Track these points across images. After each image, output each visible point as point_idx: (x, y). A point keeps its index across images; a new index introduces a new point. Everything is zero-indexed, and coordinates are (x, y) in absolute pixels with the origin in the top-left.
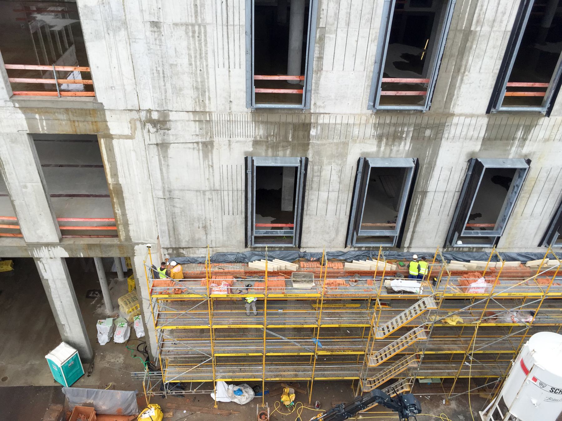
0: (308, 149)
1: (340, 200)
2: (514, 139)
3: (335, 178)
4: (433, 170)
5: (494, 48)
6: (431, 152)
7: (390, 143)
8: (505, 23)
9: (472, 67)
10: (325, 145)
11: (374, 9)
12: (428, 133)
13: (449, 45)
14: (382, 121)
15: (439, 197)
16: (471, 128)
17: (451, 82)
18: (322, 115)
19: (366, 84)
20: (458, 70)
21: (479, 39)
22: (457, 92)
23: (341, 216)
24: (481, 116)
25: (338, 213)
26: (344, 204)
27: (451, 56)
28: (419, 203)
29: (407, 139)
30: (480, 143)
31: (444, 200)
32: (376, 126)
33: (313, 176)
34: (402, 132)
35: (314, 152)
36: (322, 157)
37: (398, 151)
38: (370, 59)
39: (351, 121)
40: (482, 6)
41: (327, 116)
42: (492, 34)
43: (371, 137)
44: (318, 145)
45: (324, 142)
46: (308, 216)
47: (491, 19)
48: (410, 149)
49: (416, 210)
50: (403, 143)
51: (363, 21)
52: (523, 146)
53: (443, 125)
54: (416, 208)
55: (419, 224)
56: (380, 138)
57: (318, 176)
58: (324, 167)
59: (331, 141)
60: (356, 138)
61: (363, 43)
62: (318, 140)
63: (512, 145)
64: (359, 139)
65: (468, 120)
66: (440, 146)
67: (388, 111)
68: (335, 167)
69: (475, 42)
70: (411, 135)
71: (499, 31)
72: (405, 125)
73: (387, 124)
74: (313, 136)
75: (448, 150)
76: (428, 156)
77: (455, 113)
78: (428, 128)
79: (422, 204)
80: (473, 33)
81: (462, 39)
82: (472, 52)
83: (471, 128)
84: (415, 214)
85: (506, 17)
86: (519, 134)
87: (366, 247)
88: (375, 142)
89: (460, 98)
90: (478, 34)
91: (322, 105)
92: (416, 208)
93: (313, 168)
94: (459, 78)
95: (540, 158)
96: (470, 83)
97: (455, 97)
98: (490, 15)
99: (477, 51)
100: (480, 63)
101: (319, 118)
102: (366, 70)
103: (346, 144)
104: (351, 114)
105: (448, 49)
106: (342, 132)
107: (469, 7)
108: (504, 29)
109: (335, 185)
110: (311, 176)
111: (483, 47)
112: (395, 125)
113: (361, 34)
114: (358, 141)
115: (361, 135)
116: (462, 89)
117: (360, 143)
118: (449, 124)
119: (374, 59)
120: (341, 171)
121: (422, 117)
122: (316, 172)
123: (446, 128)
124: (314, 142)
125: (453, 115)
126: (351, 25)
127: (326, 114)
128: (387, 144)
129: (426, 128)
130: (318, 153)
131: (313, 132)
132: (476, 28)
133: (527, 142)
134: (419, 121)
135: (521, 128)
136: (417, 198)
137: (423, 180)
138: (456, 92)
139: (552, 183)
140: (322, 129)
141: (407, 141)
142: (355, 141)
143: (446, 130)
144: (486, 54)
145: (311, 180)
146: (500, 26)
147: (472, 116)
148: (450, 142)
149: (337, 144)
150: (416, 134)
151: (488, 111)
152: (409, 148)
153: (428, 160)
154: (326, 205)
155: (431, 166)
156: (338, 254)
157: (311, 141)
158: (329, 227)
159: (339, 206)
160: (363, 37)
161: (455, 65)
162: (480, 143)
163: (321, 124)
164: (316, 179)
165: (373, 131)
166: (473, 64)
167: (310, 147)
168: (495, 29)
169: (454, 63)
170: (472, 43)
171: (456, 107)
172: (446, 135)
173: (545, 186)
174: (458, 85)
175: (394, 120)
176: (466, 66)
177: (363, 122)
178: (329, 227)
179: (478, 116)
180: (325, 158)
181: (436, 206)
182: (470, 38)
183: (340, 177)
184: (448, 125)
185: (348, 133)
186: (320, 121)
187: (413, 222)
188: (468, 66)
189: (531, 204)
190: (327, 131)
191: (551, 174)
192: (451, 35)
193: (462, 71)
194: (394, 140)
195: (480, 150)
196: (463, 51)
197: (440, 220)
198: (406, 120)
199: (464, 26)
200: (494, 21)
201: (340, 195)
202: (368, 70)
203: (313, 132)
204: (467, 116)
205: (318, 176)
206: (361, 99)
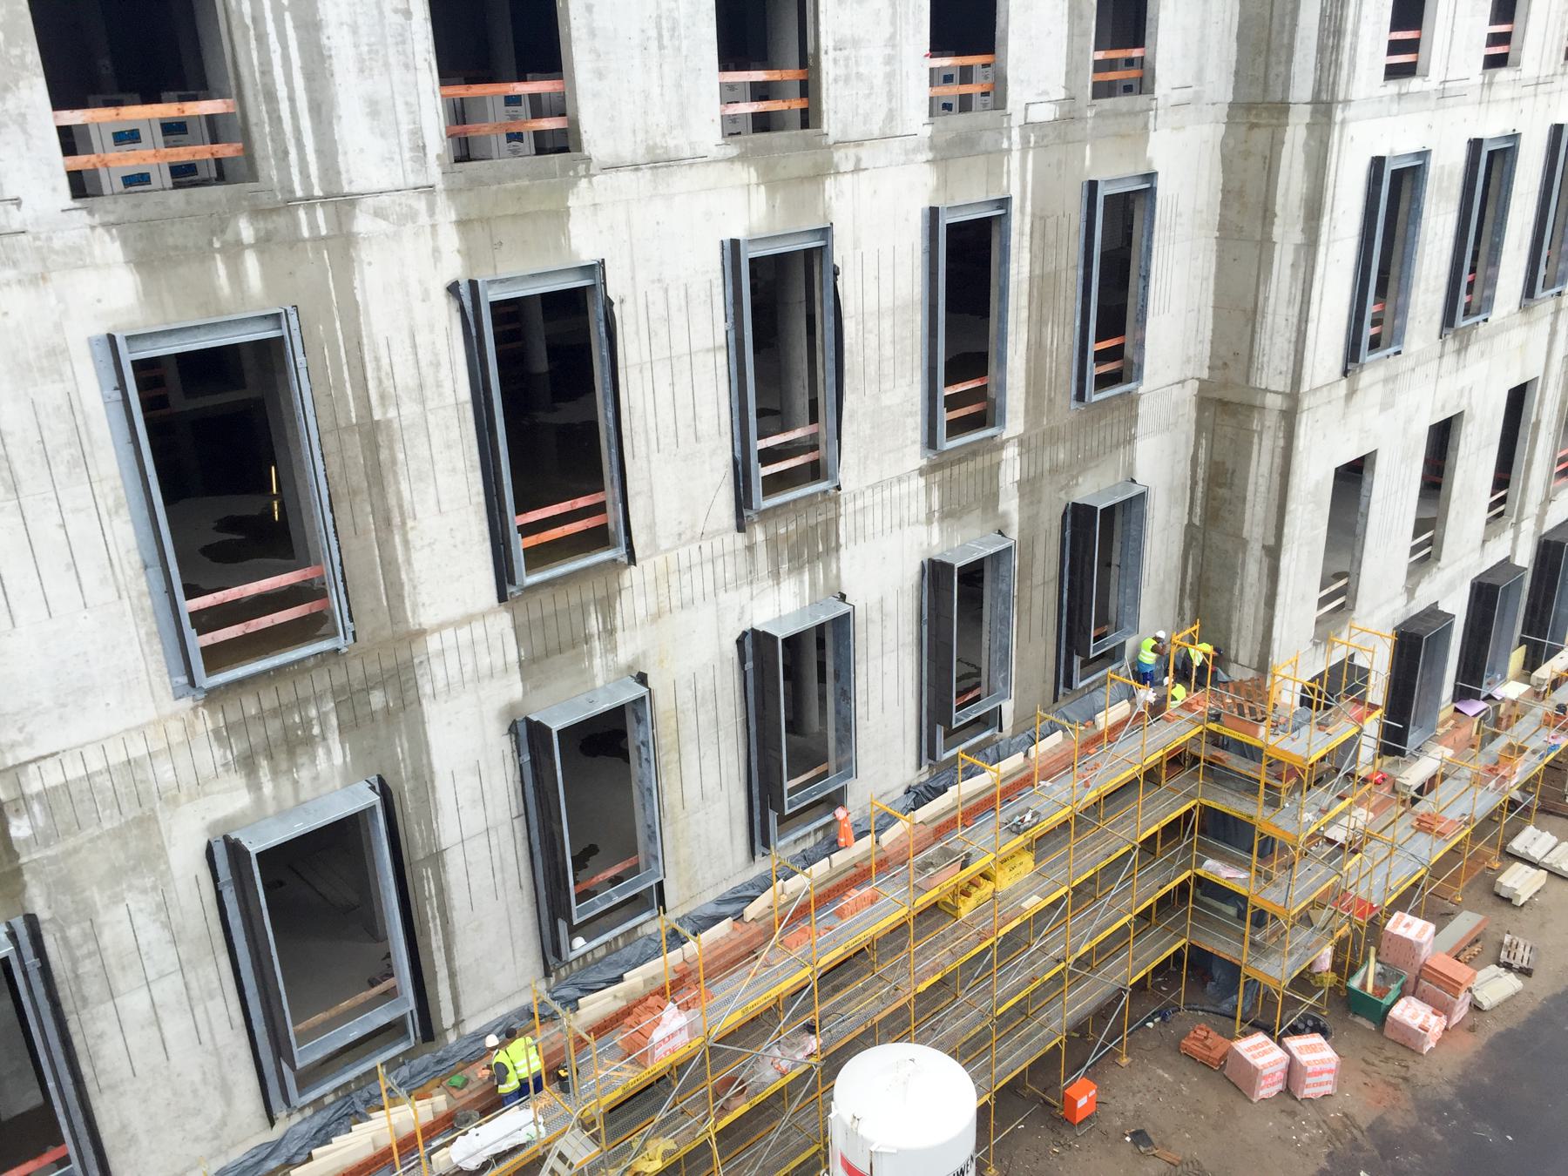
0: (24, 886)
1: (195, 992)
2: (587, 639)
3: (152, 934)
4: (433, 787)
5: (449, 447)
6: (406, 745)
7: (284, 766)
8: (448, 385)
9: (417, 507)
10: (76, 850)
11: (82, 429)
12: (377, 699)
13: (334, 469)
14: (233, 716)
15: (478, 848)
16: (481, 649)
17: (380, 556)
18: (32, 768)
19: (143, 632)
20: (385, 522)
21: (405, 437)
22: (408, 574)
23: (218, 1038)
24: (491, 611)
25: (205, 1036)
26: (212, 997)
27: (353, 492)
28: (433, 892)
29: (329, 735)
30: (517, 677)
31: (495, 853)
32: (221, 736)
33: (75, 962)
34: (306, 724)
35: (48, 886)
36: (83, 891)
37: (316, 778)
38: (126, 566)
39: (138, 750)
40: (377, 359)
41: (48, 764)
42: (431, 418)
43: (220, 769)
44: (53, 860)
45: (71, 842)
46: (107, 1096)
47: (412, 383)
48: (348, 759)
49: (433, 913)
50: (321, 752)
51: (60, 470)
52: (614, 649)
53: (409, 666)
54: (432, 908)
55: (459, 946)
56: (247, 764)
57: (90, 955)
58: (104, 918)
59: (93, 831)
60: (175, 792)
61: (83, 527)
62: (47, 846)
63: (591, 655)
64: (184, 790)
65: (464, 633)
66: (423, 723)
67: (240, 683)
68: (140, 904)
69: (398, 447)
70: (334, 721)
71: (444, 407)
72: (307, 700)
73: (254, 717)
74: (26, 840)
75: (449, 724)
76: (404, 760)
77: (424, 626)
78: (372, 688)
79: (441, 890)
80: (382, 427)
81: (362, 447)
82: (401, 470)
83: (481, 649)
84: (435, 925)
85: (445, 372)
86: (594, 624)
87: (336, 1090)
88: (238, 780)
90: (396, 425)
91: (20, 737)
92: (432, 908)
93: (65, 939)
94: (397, 539)
95: (661, 661)
96: (430, 545)
97: (407, 588)
98: (404, 376)
99: (413, 465)
100: (432, 490)
101: (23, 779)
102: (124, 594)
103: (146, 823)
104: (127, 730)
105: (337, 478)
106: (121, 790)
107: (345, 368)
108: (452, 401)
109: (163, 956)
110: (68, 965)
111: (423, 451)
112: (277, 712)
113: (66, 505)
114: (183, 798)
115: (187, 776)
116: (416, 566)
117: (191, 799)
118: (423, 658)
119: (136, 558)
120: (164, 906)
121: (343, 666)
122: (79, 946)
123: (419, 672)
124: (36, 856)
125: (421, 633)
126: (25, 489)
127: (44, 758)
128: (275, 773)
129: (367, 690)
130: (64, 884)
131: (19, 829)
132: (385, 413)
133: (619, 635)
134: (339, 678)
135: (592, 609)
136: (422, 879)
137: (419, 824)
138: (404, 576)
140: (50, 811)
141: (330, 742)
142: (174, 802)
143: (422, 676)
145: (70, 975)
146: (440, 395)
147: (469, 619)
148: (446, 702)
149: (118, 834)
150: (346, 716)
151: (502, 597)
152: (345, 756)
153: (410, 769)
154: (155, 1028)
155: (424, 780)
156: (255, 1159)
157: (23, 860)
158: (195, 1092)
159: (199, 1011)
160: (76, 511)
161: (373, 512)
162: (516, 677)
163: (38, 796)
164: (87, 967)
165: (218, 752)
167: (27, 877)
168: (430, 405)
169: (369, 509)
170: (391, 449)
171: (422, 610)
172: (426, 689)
174: (401, 558)
175: (269, 701)
176: (401, 507)
177: (176, 736)
178: (195, 1092)
180: (95, 889)
181: (481, 877)
182: (382, 439)
183: (167, 925)
184: (421, 662)
185: (140, 787)
186: (33, 786)
187: (439, 948)
188: (407, 506)
189: (691, 772)
190: (69, 809)
191: (699, 687)
192: (331, 443)
193: (396, 520)
194: (291, 753)
195: (525, 693)
196: (377, 476)
197: (507, 909)
198: (304, 687)
199: (353, 415)
200: (421, 386)
201: (190, 976)
202: (134, 594)
203: (19, 828)
204: (457, 624)
205: (90, 955)
206: (145, 678)
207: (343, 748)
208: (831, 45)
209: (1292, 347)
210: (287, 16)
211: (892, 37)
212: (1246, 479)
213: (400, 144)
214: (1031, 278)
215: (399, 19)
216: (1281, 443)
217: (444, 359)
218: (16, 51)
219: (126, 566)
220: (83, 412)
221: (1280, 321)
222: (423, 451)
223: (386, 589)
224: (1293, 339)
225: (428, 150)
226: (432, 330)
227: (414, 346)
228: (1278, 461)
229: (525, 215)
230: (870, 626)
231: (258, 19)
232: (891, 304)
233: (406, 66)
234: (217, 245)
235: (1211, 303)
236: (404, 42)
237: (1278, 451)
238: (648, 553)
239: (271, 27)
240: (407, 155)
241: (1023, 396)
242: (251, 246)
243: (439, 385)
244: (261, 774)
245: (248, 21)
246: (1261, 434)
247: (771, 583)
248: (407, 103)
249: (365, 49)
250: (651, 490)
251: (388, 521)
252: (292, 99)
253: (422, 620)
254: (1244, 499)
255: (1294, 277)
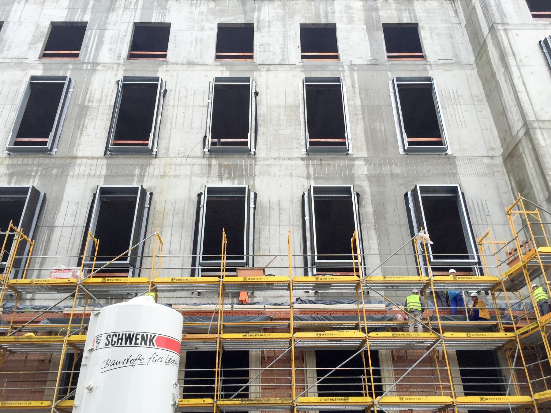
5: (103, 114)
6: (57, 188)
9: (88, 126)
12: (55, 171)
13: (69, 112)
15: (67, 232)
16: (94, 168)
19: (4, 137)
22: (78, 141)
24: (101, 158)
28: (45, 240)
30: (103, 179)
31: (73, 236)
34: (31, 171)
42: (101, 107)
48: (38, 185)
49: (42, 248)
50: (32, 180)
54: (42, 246)
65: (90, 161)
70: (39, 173)
75: (74, 186)
77: (77, 156)
78: (55, 168)
82: (87, 116)
83: (94, 168)
84: (41, 253)
85: (109, 98)
89: (81, 146)
90: (90, 107)
92: (42, 246)
95: (161, 192)
96: (88, 136)
98: (97, 97)
100: (94, 123)
102: (6, 128)
116: (82, 140)
125: (76, 158)
129: (53, 168)
133: (145, 178)
139: (181, 216)
143: (71, 169)
144: (98, 118)
147: (92, 158)
148: (76, 179)
152: (38, 184)
166: (88, 124)
170: (87, 111)
171: (78, 151)
172: (71, 174)
173: (175, 219)
179: (98, 158)
184: (73, 165)
187: (38, 262)
188: (85, 125)
191: (177, 207)
193: (81, 128)
199: (79, 103)
202: (8, 128)
204: (88, 158)
207: (38, 181)
208: (258, 44)
209: (517, 106)
210: (97, 36)
211: (284, 44)
212: (528, 177)
213: (114, 56)
214: (363, 106)
215: (123, 37)
216: (530, 146)
217: (110, 96)
218: (40, 39)
219: (10, 122)
220: (19, 92)
221: (510, 102)
222: (96, 114)
223: (70, 143)
224: (516, 104)
225: (121, 57)
226: (109, 89)
227: (102, 92)
228: (533, 155)
229: (144, 70)
230: (272, 211)
231: (90, 36)
232: (284, 105)
233: (122, 44)
234: (63, 68)
235: (493, 123)
236: (123, 40)
237: (531, 151)
238: (164, 156)
239: (92, 37)
240: (116, 57)
241: (365, 144)
242: (70, 69)
243: (106, 100)
244: (13, 180)
245: (88, 36)
246: (524, 151)
247: (218, 179)
248: (119, 49)
249: (112, 41)
250: (170, 138)
251: (78, 127)
252: (92, 48)
253: (77, 154)
254: (531, 186)
255: (507, 84)
